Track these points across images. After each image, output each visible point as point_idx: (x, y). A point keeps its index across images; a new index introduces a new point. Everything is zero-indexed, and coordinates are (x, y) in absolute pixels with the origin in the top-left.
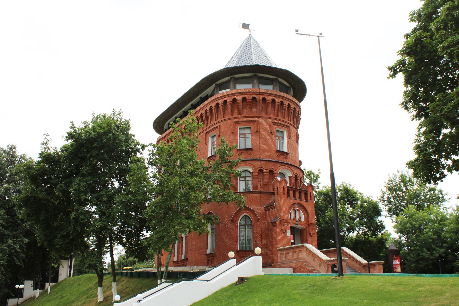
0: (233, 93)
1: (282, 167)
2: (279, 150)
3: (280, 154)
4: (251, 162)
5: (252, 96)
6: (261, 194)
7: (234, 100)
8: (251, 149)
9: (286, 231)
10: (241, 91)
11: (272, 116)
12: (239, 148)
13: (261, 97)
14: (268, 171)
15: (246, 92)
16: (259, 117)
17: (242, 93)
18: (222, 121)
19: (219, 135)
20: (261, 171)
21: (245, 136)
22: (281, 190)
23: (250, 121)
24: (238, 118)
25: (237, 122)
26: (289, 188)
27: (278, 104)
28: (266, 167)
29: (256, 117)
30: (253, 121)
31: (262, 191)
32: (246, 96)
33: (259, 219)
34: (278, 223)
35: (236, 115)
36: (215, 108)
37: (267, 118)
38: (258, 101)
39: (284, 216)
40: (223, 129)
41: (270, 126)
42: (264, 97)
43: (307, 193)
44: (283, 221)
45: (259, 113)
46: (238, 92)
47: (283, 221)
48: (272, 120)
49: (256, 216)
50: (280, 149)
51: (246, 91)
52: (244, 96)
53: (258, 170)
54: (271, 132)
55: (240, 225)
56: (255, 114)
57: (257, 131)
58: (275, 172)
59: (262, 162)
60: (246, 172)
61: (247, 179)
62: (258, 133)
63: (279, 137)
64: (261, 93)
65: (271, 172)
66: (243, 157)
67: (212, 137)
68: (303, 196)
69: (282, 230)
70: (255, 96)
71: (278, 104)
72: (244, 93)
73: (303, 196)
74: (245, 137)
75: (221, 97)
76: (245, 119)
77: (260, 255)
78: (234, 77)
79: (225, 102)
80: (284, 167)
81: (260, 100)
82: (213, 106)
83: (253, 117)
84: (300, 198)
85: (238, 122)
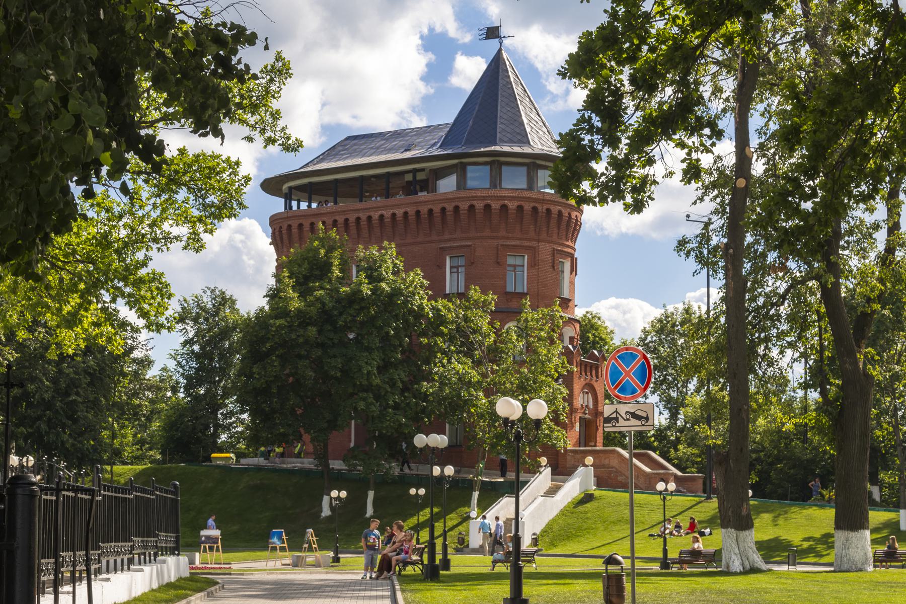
5: (532, 205)
13: (545, 207)
15: (523, 197)
16: (538, 241)
21: (515, 269)
23: (526, 246)
24: (508, 238)
25: (506, 245)
36: (466, 212)
37: (549, 242)
38: (540, 214)
41: (553, 255)
70: (536, 205)
72: (521, 197)
76: (518, 243)
77: (591, 466)
83: (529, 240)
85: (508, 245)
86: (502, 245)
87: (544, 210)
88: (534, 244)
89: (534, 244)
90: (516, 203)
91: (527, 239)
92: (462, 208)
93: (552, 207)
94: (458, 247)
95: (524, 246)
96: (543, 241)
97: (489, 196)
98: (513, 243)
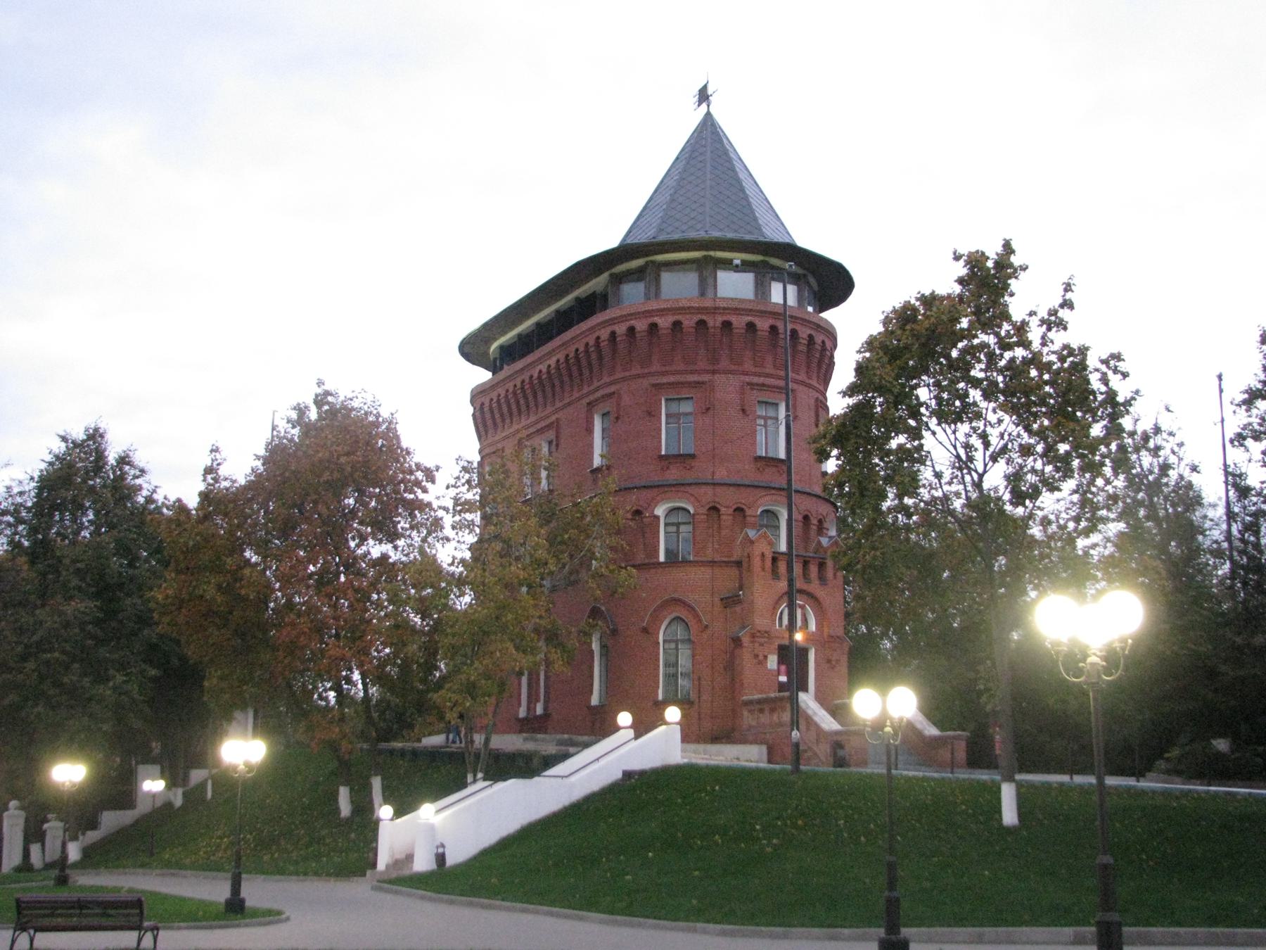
1: (767, 498)
2: (764, 455)
3: (767, 465)
4: (688, 489)
5: (696, 318)
6: (712, 566)
7: (653, 327)
8: (692, 456)
9: (766, 657)
10: (669, 306)
11: (748, 366)
12: (663, 453)
13: (720, 319)
14: (730, 511)
16: (714, 372)
18: (624, 379)
19: (616, 415)
20: (714, 509)
22: (757, 561)
24: (664, 374)
26: (776, 555)
27: (764, 333)
28: (727, 499)
29: (707, 372)
31: (716, 560)
33: (706, 627)
34: (746, 640)
35: (656, 367)
39: (760, 622)
40: (626, 400)
41: (742, 393)
43: (825, 563)
44: (758, 634)
45: (714, 360)
47: (758, 634)
48: (747, 379)
49: (700, 621)
50: (766, 452)
51: (681, 305)
53: (707, 508)
54: (743, 411)
55: (664, 641)
56: (702, 364)
57: (708, 409)
58: (748, 512)
59: (719, 490)
60: (680, 512)
61: (682, 528)
62: (711, 412)
63: (765, 418)
65: (739, 510)
66: (674, 474)
67: (604, 415)
68: (814, 569)
69: (756, 656)
70: (704, 317)
71: (764, 333)
73: (814, 569)
74: (678, 423)
78: (653, 262)
79: (632, 330)
80: (774, 497)
81: (714, 327)
82: (603, 338)
84: (806, 575)
86: (654, 385)
87: (718, 324)
88: (705, 378)
89: (705, 378)
90: (671, 319)
91: (692, 372)
93: (734, 319)
97: (632, 314)
98: (672, 379)
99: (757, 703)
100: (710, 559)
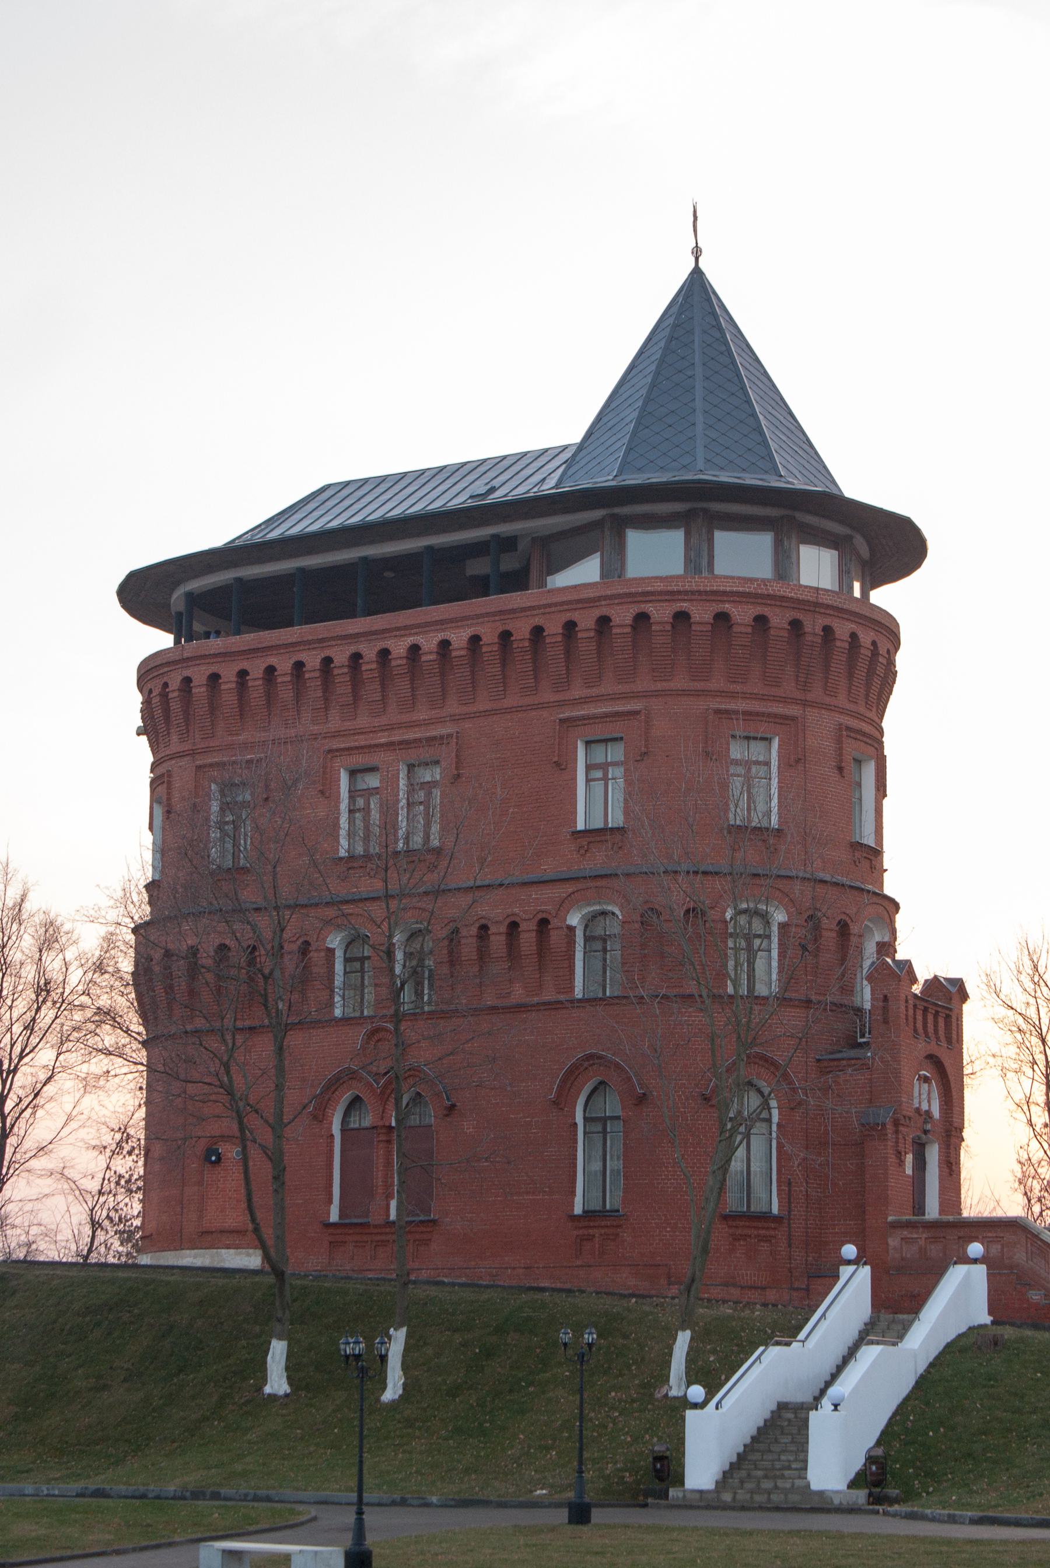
0: (721, 588)
11: (842, 700)
13: (821, 621)
15: (769, 596)
16: (805, 704)
17: (756, 596)
23: (775, 716)
24: (733, 695)
29: (794, 701)
30: (785, 717)
32: (766, 611)
35: (718, 683)
37: (829, 708)
41: (839, 741)
42: (827, 621)
46: (741, 589)
52: (759, 610)
57: (798, 761)
64: (822, 605)
72: (763, 596)
75: (661, 593)
83: (785, 700)
86: (718, 712)
88: (793, 711)
89: (793, 711)
91: (775, 699)
92: (616, 620)
94: (606, 715)
95: (769, 715)
96: (814, 704)
97: (686, 592)
99: (924, 1227)
100: (803, 998)
